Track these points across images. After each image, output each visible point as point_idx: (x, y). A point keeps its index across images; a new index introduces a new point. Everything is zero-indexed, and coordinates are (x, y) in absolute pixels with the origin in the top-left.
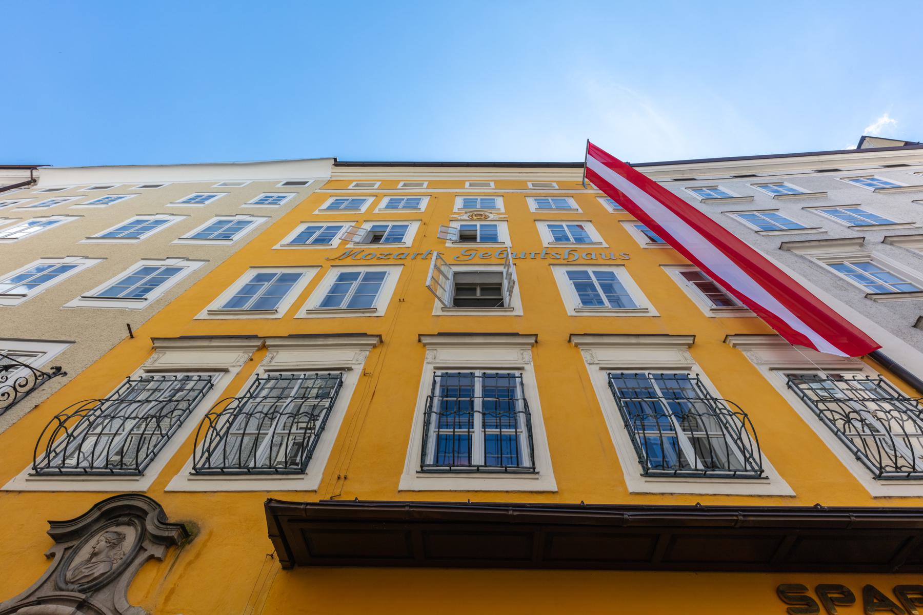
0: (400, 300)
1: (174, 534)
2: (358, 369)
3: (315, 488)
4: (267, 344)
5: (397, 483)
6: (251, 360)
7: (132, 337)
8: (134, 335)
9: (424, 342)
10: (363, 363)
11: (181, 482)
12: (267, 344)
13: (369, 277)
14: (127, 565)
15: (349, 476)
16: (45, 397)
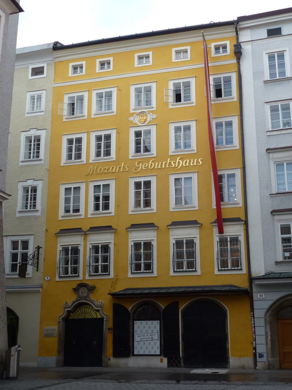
0: (118, 206)
1: (93, 289)
2: (113, 241)
3: (113, 278)
4: (86, 233)
5: (127, 276)
6: (84, 239)
7: (47, 231)
8: (47, 230)
9: (128, 230)
10: (113, 239)
11: (87, 277)
12: (86, 233)
13: (104, 185)
14: (88, 294)
15: (118, 275)
16: (43, 256)
